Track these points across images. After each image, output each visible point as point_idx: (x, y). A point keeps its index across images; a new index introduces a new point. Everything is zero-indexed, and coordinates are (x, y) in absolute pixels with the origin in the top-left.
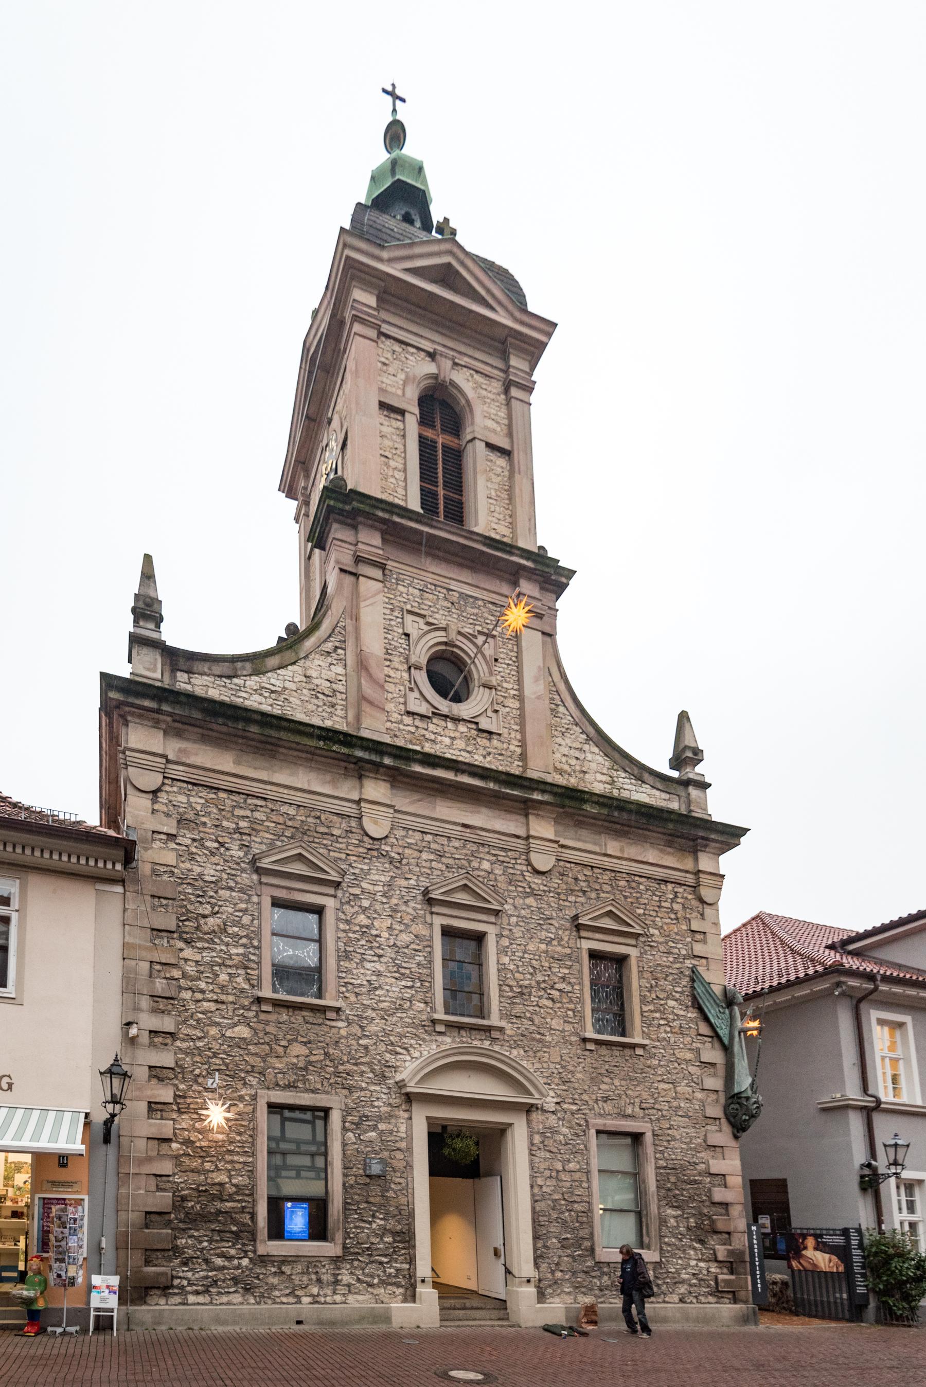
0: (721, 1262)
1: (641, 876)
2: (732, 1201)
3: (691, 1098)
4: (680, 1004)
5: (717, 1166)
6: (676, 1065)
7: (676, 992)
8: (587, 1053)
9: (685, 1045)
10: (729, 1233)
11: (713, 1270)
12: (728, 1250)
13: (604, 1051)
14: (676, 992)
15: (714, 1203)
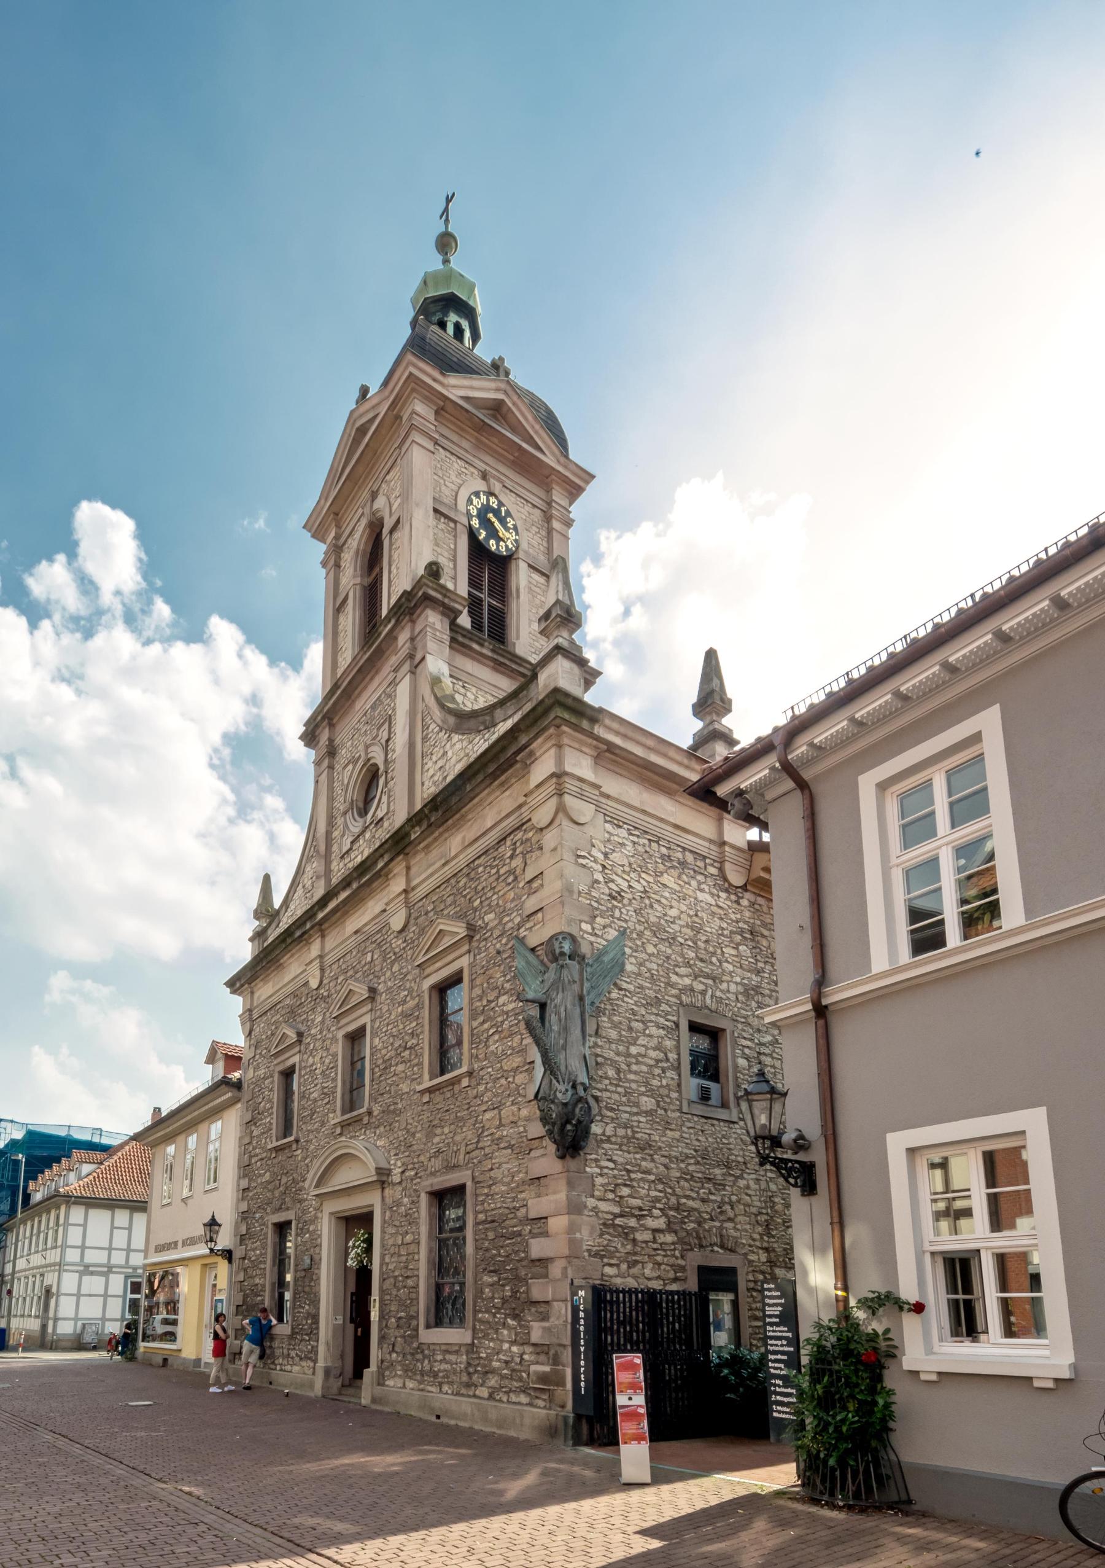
0: (534, 1345)
1: (479, 857)
2: (551, 1255)
3: (515, 1119)
4: (512, 995)
5: (537, 1206)
6: (503, 1081)
7: (508, 981)
8: (425, 1107)
9: (513, 1049)
10: (547, 1302)
11: (526, 1357)
12: (544, 1328)
13: (438, 1097)
14: (508, 981)
15: (532, 1261)
